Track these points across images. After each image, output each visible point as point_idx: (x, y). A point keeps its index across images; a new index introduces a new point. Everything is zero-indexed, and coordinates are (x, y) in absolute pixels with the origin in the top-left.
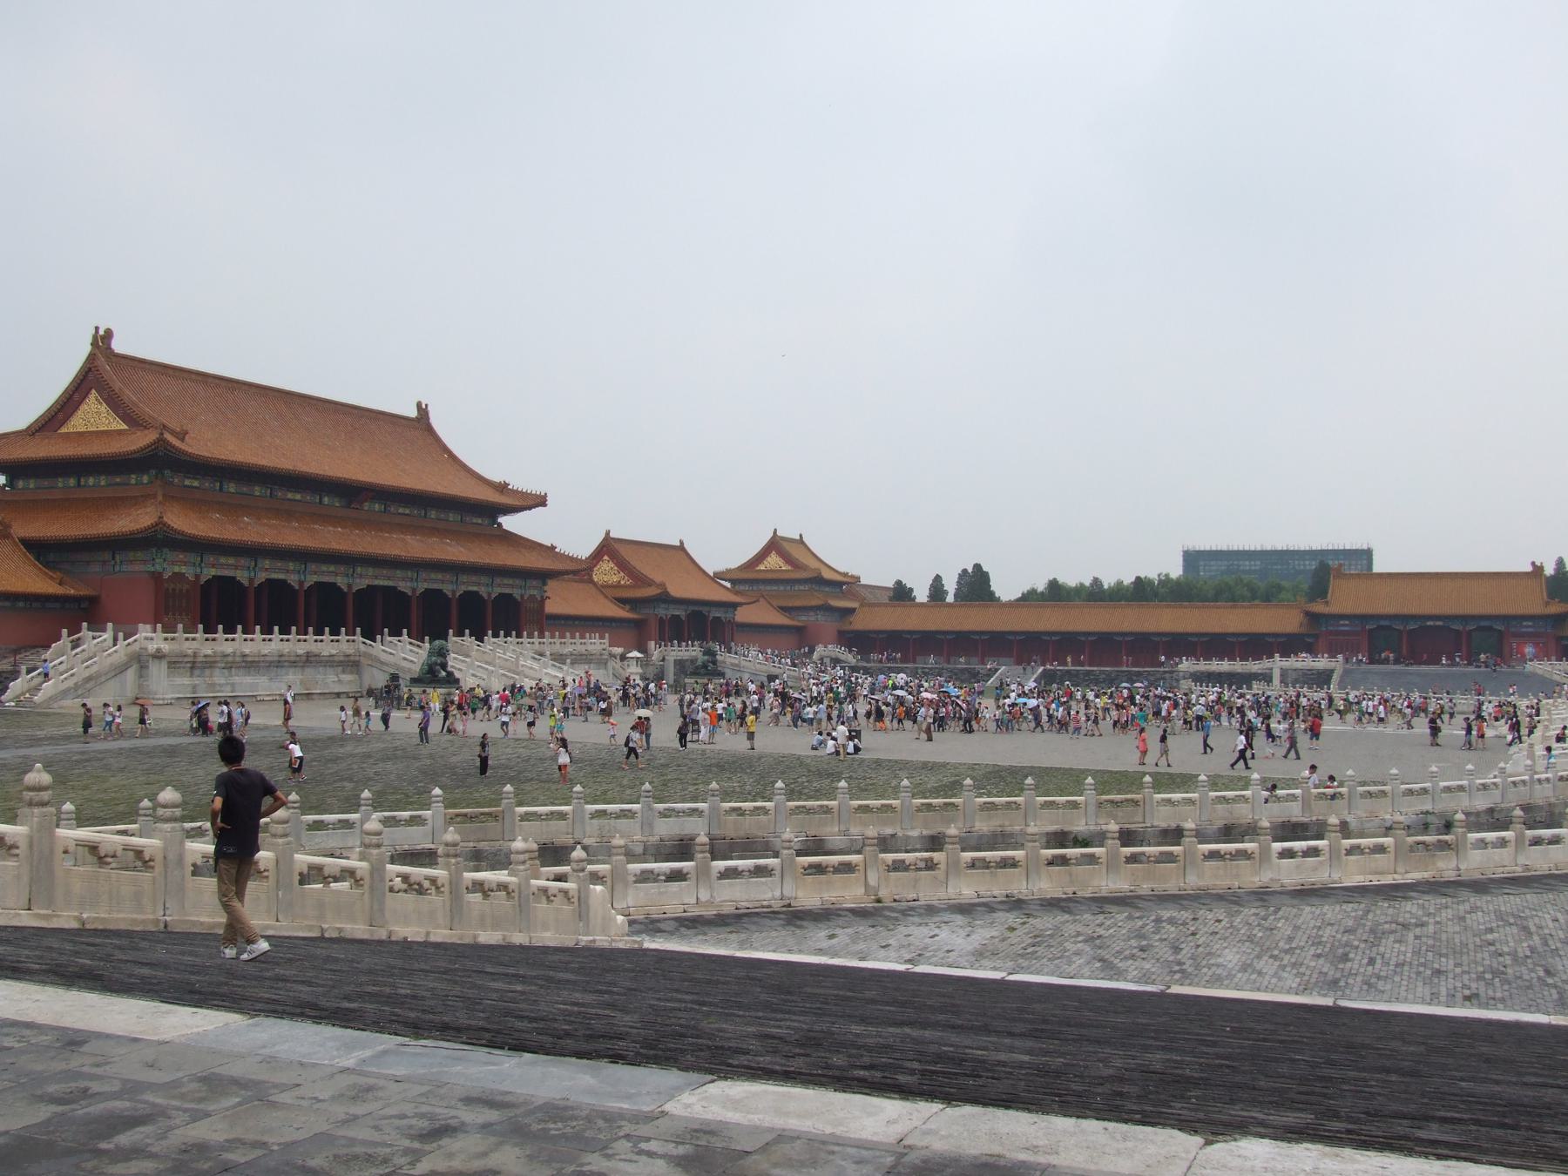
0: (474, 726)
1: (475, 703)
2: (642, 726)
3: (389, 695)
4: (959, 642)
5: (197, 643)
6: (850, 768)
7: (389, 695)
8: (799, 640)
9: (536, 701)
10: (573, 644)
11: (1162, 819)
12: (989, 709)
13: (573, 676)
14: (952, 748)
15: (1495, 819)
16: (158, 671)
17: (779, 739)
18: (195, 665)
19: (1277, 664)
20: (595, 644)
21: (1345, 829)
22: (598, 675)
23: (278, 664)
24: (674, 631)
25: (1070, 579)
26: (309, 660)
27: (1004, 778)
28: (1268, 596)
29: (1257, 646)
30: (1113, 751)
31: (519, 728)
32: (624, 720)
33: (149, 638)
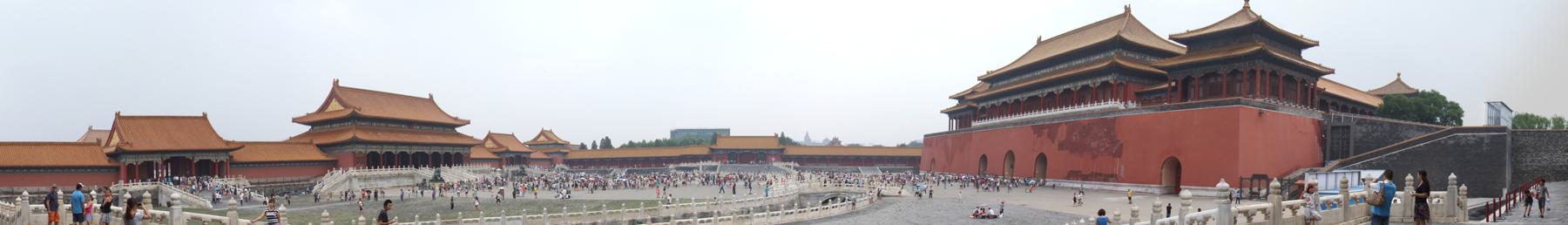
0: (449, 194)
1: (449, 187)
2: (501, 192)
3: (423, 185)
4: (601, 162)
5: (366, 172)
6: (575, 206)
7: (423, 185)
8: (551, 163)
9: (469, 185)
10: (479, 167)
11: (664, 213)
12: (611, 182)
13: (479, 177)
14: (600, 195)
15: (762, 209)
16: (355, 181)
17: (544, 195)
18: (366, 179)
19: (701, 164)
20: (486, 167)
21: (719, 214)
22: (488, 177)
23: (390, 177)
24: (511, 162)
25: (636, 141)
26: (399, 176)
27: (616, 204)
28: (699, 143)
29: (695, 158)
30: (649, 194)
31: (463, 194)
32: (496, 190)
33: (352, 171)
